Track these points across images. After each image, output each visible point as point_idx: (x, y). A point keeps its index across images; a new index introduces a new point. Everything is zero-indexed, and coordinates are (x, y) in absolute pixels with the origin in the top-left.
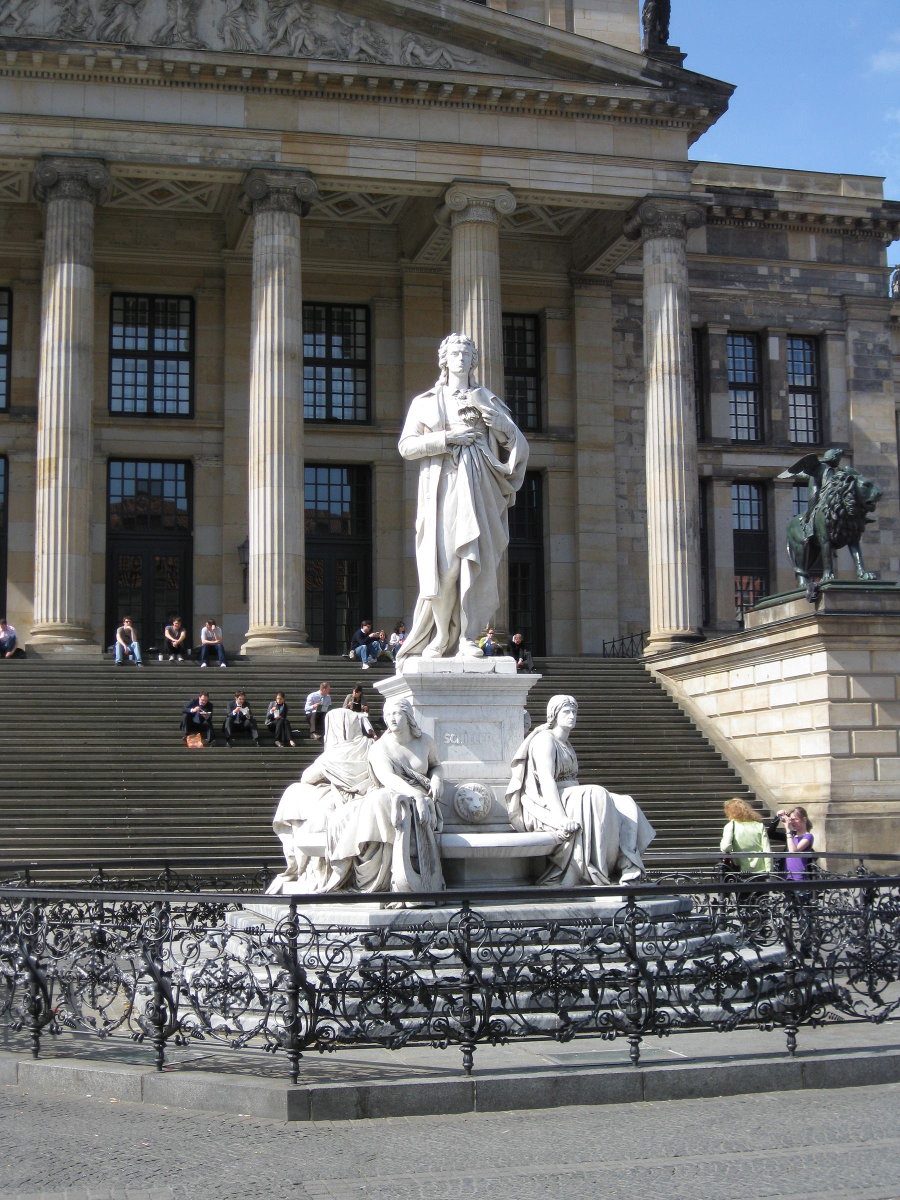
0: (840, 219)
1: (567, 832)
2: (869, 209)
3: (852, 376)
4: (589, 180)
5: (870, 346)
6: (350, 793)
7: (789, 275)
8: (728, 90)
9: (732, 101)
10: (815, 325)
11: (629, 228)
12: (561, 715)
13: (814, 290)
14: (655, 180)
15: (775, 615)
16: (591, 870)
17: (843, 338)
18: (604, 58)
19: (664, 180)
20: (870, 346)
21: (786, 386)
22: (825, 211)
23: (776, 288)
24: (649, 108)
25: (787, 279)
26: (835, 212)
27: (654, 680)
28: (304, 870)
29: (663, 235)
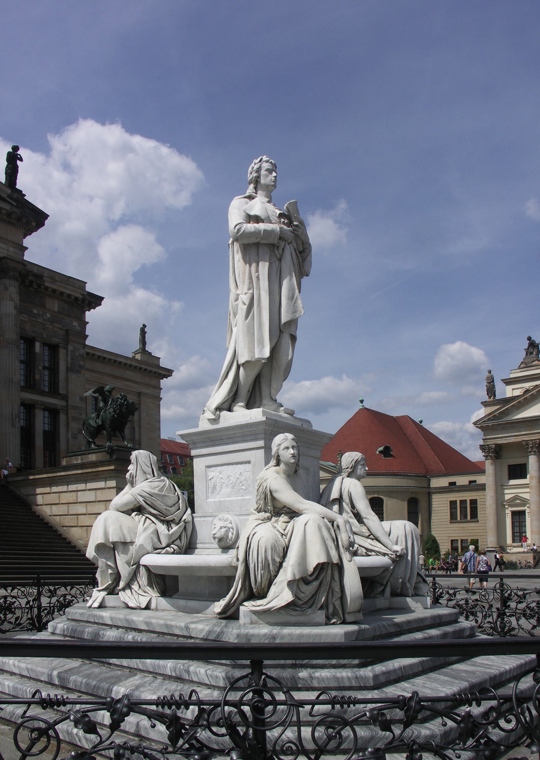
2: (82, 294)
3: (69, 366)
5: (77, 354)
7: (46, 316)
10: (55, 340)
13: (55, 325)
17: (66, 349)
20: (77, 354)
22: (64, 291)
23: (40, 320)
25: (45, 317)
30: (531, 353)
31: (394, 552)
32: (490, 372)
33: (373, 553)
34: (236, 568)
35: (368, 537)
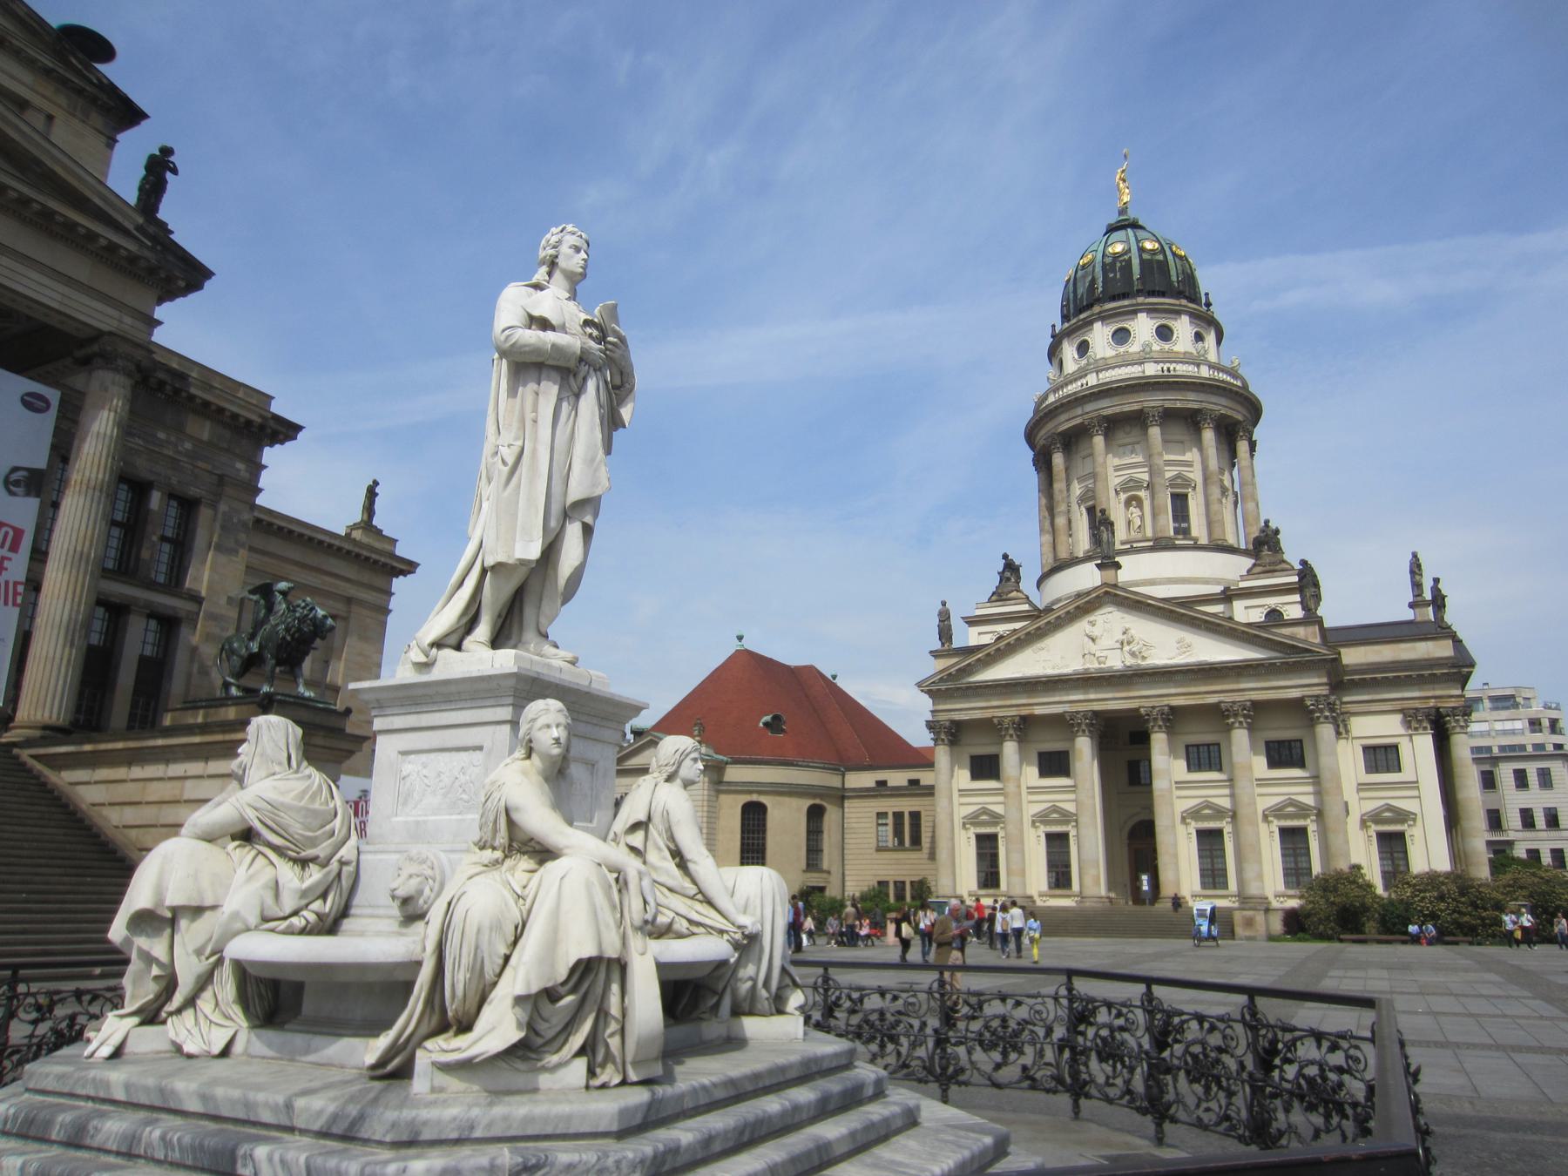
0: (235, 416)
1: (745, 936)
4: (59, 297)
6: (295, 861)
8: (207, 274)
9: (208, 284)
10: (193, 491)
11: (80, 353)
12: (688, 762)
13: (200, 464)
14: (120, 321)
15: (205, 716)
16: (764, 993)
17: (214, 506)
18: (104, 199)
19: (128, 324)
21: (159, 533)
24: (133, 259)
26: (235, 409)
27: (24, 764)
28: (191, 1002)
29: (116, 370)
30: (1008, 579)
31: (740, 927)
32: (944, 604)
33: (701, 930)
34: (419, 964)
35: (692, 898)
